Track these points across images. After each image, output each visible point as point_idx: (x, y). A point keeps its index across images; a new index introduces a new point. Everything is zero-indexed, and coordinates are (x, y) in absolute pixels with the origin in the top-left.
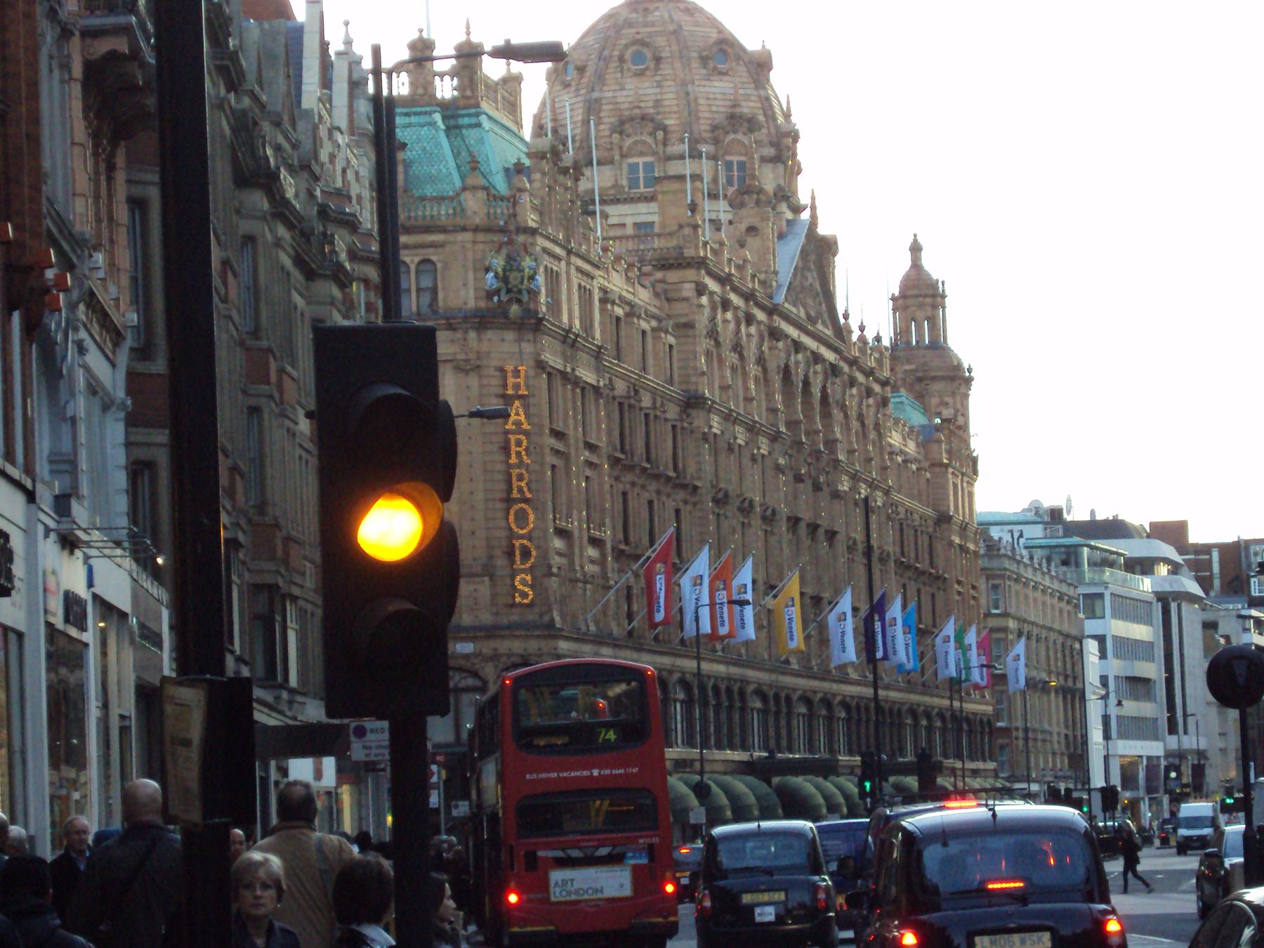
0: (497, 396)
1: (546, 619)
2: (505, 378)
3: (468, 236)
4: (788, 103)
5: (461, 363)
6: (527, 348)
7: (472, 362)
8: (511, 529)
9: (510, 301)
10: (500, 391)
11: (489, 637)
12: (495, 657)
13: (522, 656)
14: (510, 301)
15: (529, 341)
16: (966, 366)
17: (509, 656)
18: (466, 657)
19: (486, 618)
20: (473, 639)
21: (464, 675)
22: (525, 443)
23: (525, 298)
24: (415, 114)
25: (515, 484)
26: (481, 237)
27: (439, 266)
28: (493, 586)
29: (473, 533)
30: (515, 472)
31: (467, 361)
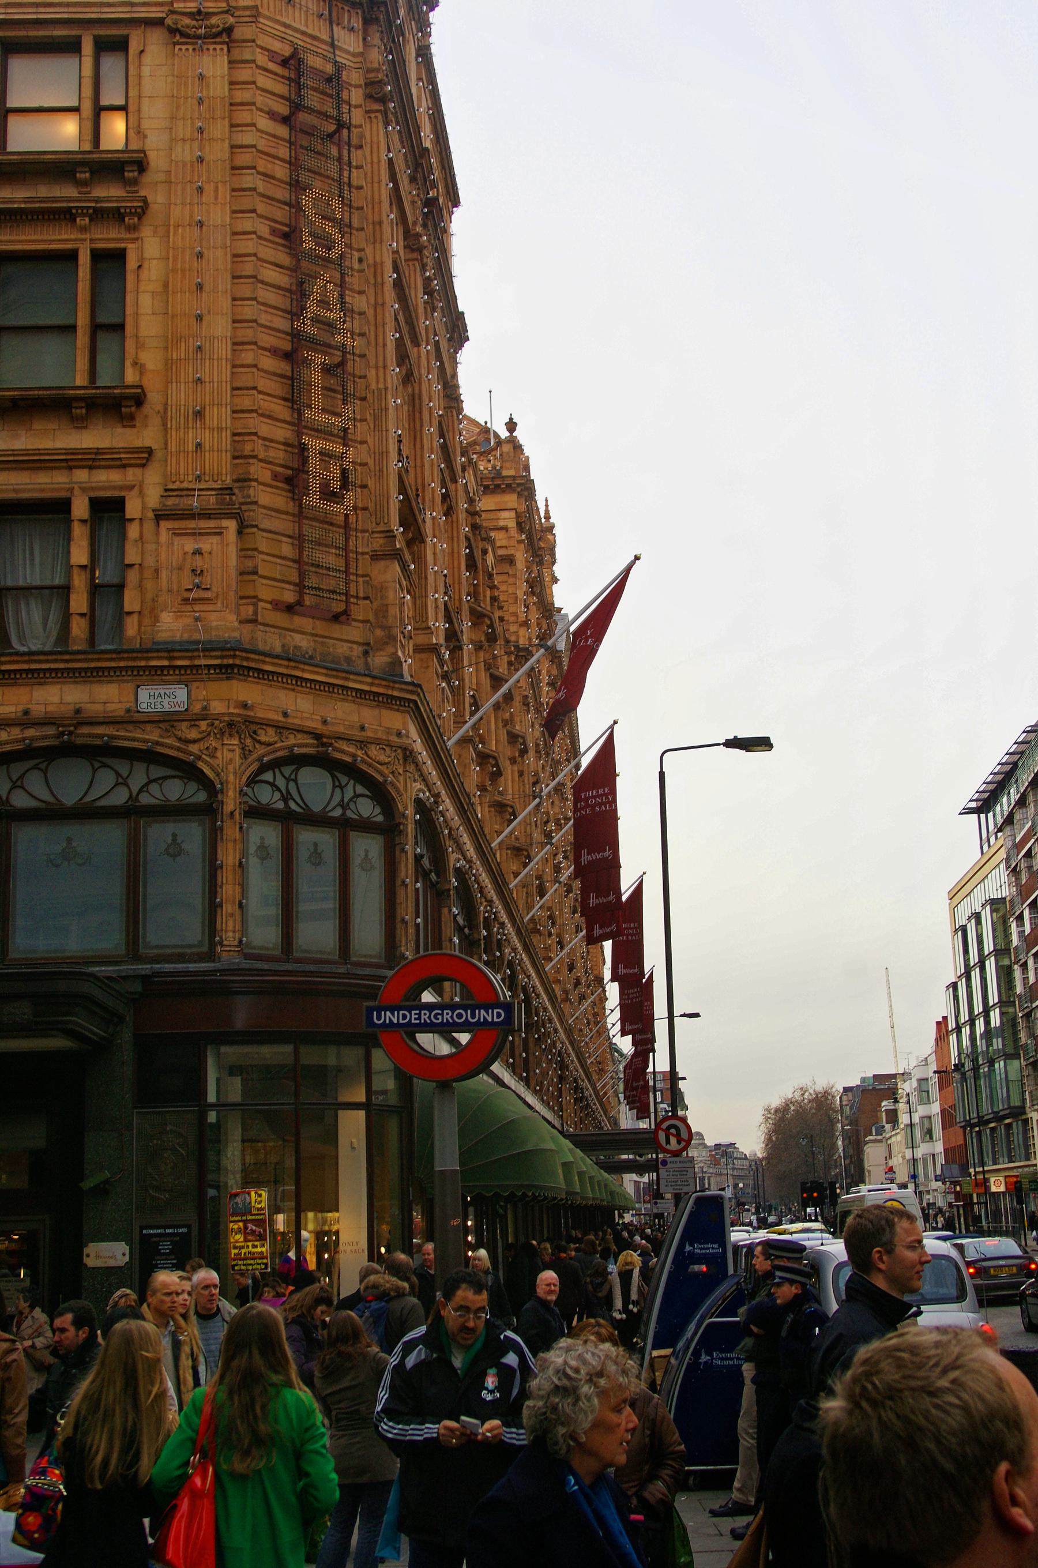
0: (272, 115)
1: (379, 660)
4: (547, 506)
5: (187, 21)
6: (349, 42)
7: (214, 21)
10: (283, 109)
11: (226, 671)
13: (318, 736)
15: (352, 29)
17: (280, 728)
18: (168, 720)
20: (187, 675)
21: (157, 771)
28: (246, 552)
29: (199, 414)
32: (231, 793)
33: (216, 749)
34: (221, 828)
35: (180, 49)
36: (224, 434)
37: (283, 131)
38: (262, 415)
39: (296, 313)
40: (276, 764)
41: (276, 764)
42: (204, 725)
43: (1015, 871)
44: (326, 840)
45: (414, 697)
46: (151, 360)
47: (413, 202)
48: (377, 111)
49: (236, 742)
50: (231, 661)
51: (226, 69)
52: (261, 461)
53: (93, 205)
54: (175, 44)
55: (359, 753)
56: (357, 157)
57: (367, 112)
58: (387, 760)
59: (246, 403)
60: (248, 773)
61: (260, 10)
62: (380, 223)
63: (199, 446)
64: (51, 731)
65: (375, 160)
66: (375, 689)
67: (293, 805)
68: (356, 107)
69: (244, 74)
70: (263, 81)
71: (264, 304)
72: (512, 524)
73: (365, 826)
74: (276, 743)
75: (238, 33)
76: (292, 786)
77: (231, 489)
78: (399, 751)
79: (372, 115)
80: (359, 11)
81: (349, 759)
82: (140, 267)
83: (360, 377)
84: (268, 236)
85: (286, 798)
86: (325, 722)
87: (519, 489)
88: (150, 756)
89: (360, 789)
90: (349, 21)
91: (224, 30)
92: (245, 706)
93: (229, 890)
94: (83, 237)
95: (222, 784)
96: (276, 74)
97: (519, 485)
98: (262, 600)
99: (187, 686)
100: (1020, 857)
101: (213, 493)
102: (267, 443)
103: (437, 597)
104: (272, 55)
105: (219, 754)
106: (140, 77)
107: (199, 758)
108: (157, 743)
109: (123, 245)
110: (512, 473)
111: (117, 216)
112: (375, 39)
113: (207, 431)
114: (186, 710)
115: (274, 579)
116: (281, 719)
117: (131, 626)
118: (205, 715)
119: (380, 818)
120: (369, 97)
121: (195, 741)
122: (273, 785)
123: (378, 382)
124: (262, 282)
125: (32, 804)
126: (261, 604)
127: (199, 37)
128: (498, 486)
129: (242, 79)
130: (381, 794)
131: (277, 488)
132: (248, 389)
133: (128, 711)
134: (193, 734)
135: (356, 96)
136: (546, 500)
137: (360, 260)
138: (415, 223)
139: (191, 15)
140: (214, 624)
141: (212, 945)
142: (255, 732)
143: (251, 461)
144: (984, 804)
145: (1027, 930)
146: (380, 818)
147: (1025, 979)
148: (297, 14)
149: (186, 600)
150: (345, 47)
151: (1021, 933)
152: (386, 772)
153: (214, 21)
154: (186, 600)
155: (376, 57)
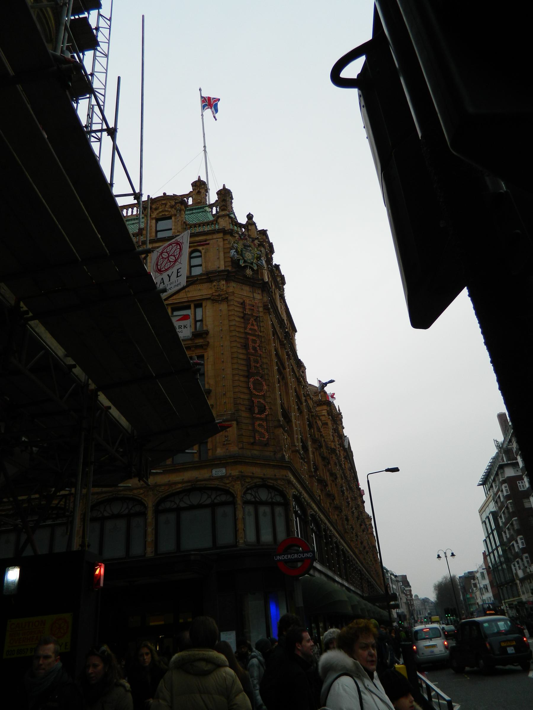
0: (239, 317)
1: (279, 456)
2: (244, 309)
3: (221, 235)
4: (339, 408)
5: (216, 297)
6: (258, 296)
7: (223, 296)
8: (251, 393)
9: (246, 267)
10: (242, 315)
12: (242, 478)
14: (246, 267)
15: (259, 294)
16: (370, 516)
17: (251, 477)
18: (221, 478)
19: (234, 449)
22: (258, 342)
23: (255, 268)
24: (195, 209)
25: (253, 364)
26: (228, 237)
27: (203, 251)
29: (225, 394)
30: (252, 358)
31: (219, 295)
32: (239, 497)
33: (234, 485)
34: (237, 507)
35: (215, 304)
36: (231, 398)
37: (242, 320)
38: (241, 393)
39: (249, 366)
40: (250, 488)
41: (250, 488)
42: (230, 479)
43: (496, 502)
44: (266, 509)
45: (290, 465)
46: (212, 382)
47: (281, 333)
48: (267, 312)
49: (239, 483)
50: (236, 460)
51: (227, 307)
52: (242, 405)
53: (195, 345)
54: (214, 303)
55: (275, 482)
56: (262, 324)
57: (265, 313)
58: (283, 484)
59: (237, 390)
60: (244, 491)
61: (235, 292)
62: (270, 340)
63: (225, 402)
64: (190, 484)
65: (267, 324)
66: (278, 464)
67: (257, 499)
68: (261, 312)
69: (231, 308)
70: (236, 309)
71: (240, 364)
72: (326, 414)
73: (278, 504)
74: (251, 482)
75: (229, 298)
76: (257, 495)
77: (234, 413)
78: (286, 481)
79: (266, 313)
80: (260, 289)
81: (271, 484)
82: (208, 358)
83: (267, 380)
84: (240, 347)
85: (255, 497)
86: (264, 475)
87: (327, 404)
88: (216, 489)
89: (276, 493)
90: (258, 291)
91: (226, 298)
92: (241, 472)
93: (240, 526)
94: (193, 353)
95: (236, 495)
96: (240, 307)
97: (327, 403)
98: (244, 442)
99: (225, 468)
100: (497, 498)
101: (229, 415)
102: (243, 400)
103: (297, 436)
104: (238, 302)
105: (235, 486)
106: (206, 312)
107: (230, 488)
108: (218, 485)
109: (203, 354)
110: (324, 400)
111: (201, 347)
112: (265, 295)
113: (227, 399)
114: (225, 475)
115: (248, 436)
116: (252, 475)
117: (210, 453)
118: (230, 476)
119: (282, 501)
120: (264, 309)
121: (228, 483)
122: (251, 494)
123: (272, 380)
124: (239, 358)
125: (185, 505)
126: (244, 444)
127: (220, 301)
128: (321, 404)
129: (231, 309)
130: (283, 495)
131: (247, 411)
132: (237, 386)
133: (210, 476)
134: (228, 482)
135: (261, 309)
136: (338, 406)
137: (265, 350)
138: (282, 338)
139: (217, 296)
140: (232, 450)
141: (236, 542)
142: (245, 479)
143: (239, 405)
144: (484, 482)
145: (504, 520)
146: (282, 501)
147: (506, 537)
148: (244, 291)
149: (224, 445)
150: (258, 298)
151: (502, 522)
152: (283, 487)
153: (223, 296)
154: (224, 445)
155: (265, 299)
